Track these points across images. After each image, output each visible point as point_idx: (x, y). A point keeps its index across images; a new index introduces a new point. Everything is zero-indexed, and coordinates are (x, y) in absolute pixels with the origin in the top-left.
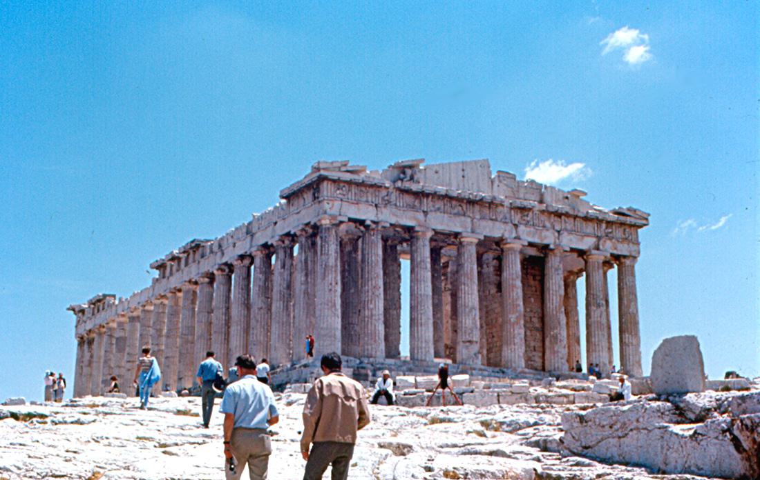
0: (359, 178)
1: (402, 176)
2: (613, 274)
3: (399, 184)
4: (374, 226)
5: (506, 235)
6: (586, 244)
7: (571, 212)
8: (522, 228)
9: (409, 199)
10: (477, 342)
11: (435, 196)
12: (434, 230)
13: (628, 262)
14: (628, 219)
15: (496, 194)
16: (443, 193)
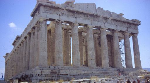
0: (53, 5)
1: (68, 5)
2: (131, 39)
3: (67, 8)
4: (58, 21)
5: (102, 26)
6: (124, 29)
7: (120, 20)
8: (106, 24)
9: (71, 14)
10: (94, 59)
11: (78, 13)
12: (79, 23)
13: (135, 35)
14: (135, 22)
15: (98, 13)
16: (81, 12)
